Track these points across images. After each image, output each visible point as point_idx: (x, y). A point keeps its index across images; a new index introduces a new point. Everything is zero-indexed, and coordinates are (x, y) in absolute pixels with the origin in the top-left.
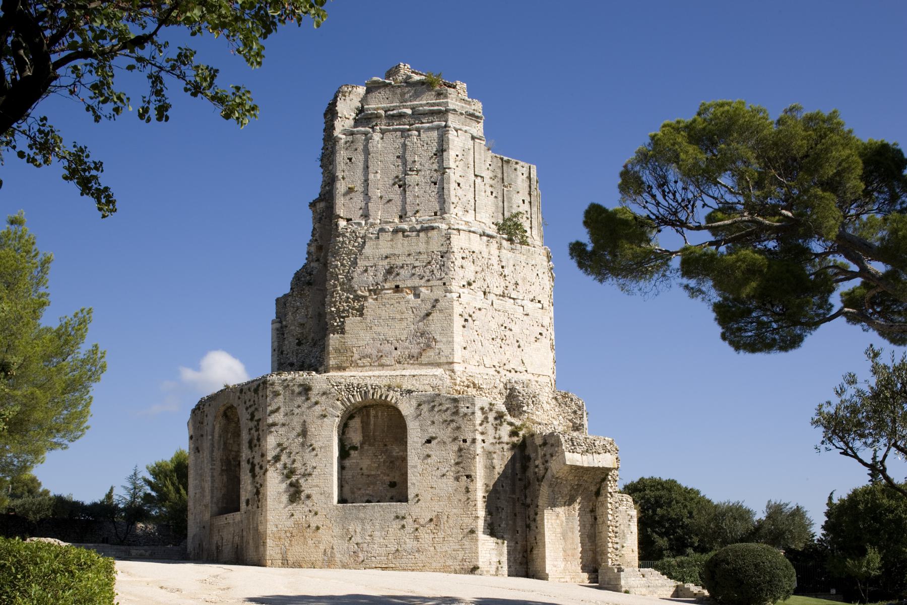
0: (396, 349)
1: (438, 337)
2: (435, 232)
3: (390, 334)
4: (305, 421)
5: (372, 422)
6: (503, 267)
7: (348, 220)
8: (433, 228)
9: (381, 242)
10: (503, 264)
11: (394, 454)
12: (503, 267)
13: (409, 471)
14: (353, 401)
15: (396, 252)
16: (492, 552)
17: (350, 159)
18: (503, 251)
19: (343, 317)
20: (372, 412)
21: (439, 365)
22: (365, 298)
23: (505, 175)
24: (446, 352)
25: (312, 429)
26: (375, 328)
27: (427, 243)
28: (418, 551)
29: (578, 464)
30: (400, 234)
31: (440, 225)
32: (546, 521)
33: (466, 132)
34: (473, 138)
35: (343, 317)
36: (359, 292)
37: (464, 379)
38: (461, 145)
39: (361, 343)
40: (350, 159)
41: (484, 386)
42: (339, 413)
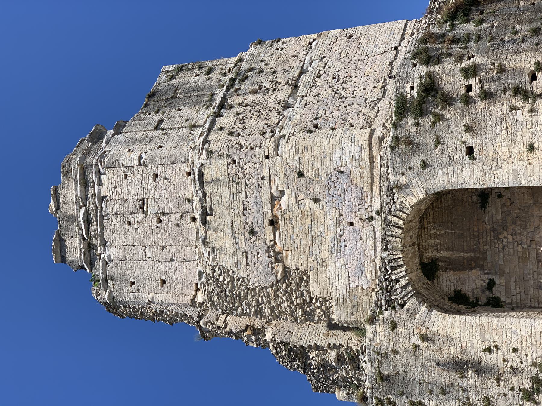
0: (352, 224)
1: (335, 164)
2: (205, 171)
3: (331, 232)
4: (438, 364)
5: (446, 254)
7: (197, 289)
8: (201, 175)
9: (217, 245)
11: (499, 217)
13: (525, 184)
14: (403, 282)
15: (230, 224)
17: (133, 283)
19: (311, 299)
20: (431, 254)
21: (372, 161)
22: (285, 268)
25: (451, 352)
26: (324, 254)
27: (216, 181)
30: (209, 218)
31: (198, 166)
33: (107, 143)
35: (311, 299)
36: (279, 276)
39: (345, 275)
40: (133, 283)
42: (424, 309)
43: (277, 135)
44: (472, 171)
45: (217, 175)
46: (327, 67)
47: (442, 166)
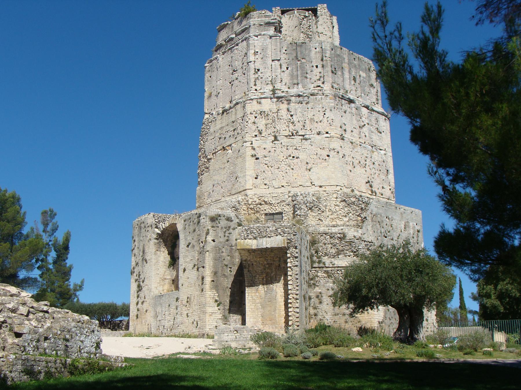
6: (292, 116)
10: (292, 113)
12: (292, 116)
16: (219, 321)
18: (292, 104)
23: (299, 53)
24: (243, 184)
25: (146, 250)
28: (182, 323)
29: (248, 247)
32: (247, 294)
33: (264, 35)
34: (271, 37)
37: (255, 199)
38: (261, 44)
41: (274, 202)
43: (253, 140)
44: (183, 248)
45: (238, 112)
46: (304, 150)
47: (185, 236)
